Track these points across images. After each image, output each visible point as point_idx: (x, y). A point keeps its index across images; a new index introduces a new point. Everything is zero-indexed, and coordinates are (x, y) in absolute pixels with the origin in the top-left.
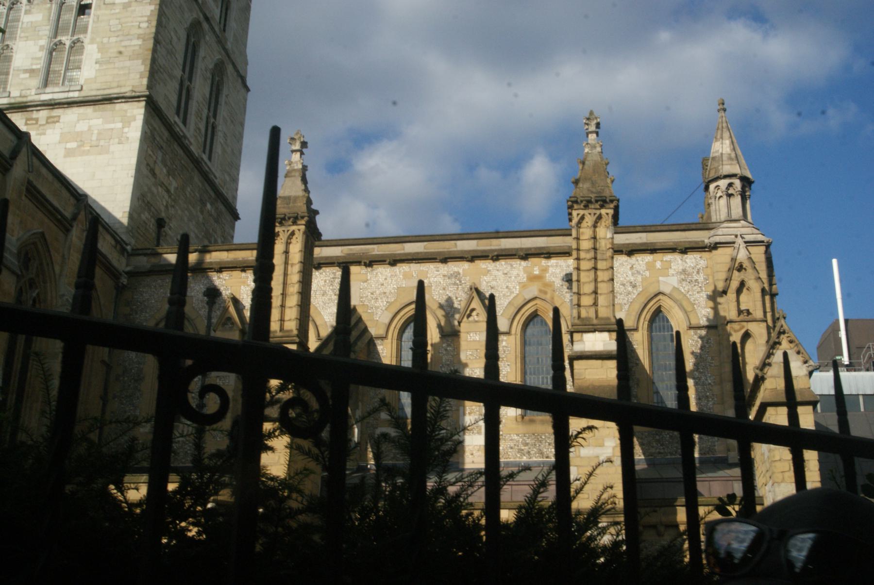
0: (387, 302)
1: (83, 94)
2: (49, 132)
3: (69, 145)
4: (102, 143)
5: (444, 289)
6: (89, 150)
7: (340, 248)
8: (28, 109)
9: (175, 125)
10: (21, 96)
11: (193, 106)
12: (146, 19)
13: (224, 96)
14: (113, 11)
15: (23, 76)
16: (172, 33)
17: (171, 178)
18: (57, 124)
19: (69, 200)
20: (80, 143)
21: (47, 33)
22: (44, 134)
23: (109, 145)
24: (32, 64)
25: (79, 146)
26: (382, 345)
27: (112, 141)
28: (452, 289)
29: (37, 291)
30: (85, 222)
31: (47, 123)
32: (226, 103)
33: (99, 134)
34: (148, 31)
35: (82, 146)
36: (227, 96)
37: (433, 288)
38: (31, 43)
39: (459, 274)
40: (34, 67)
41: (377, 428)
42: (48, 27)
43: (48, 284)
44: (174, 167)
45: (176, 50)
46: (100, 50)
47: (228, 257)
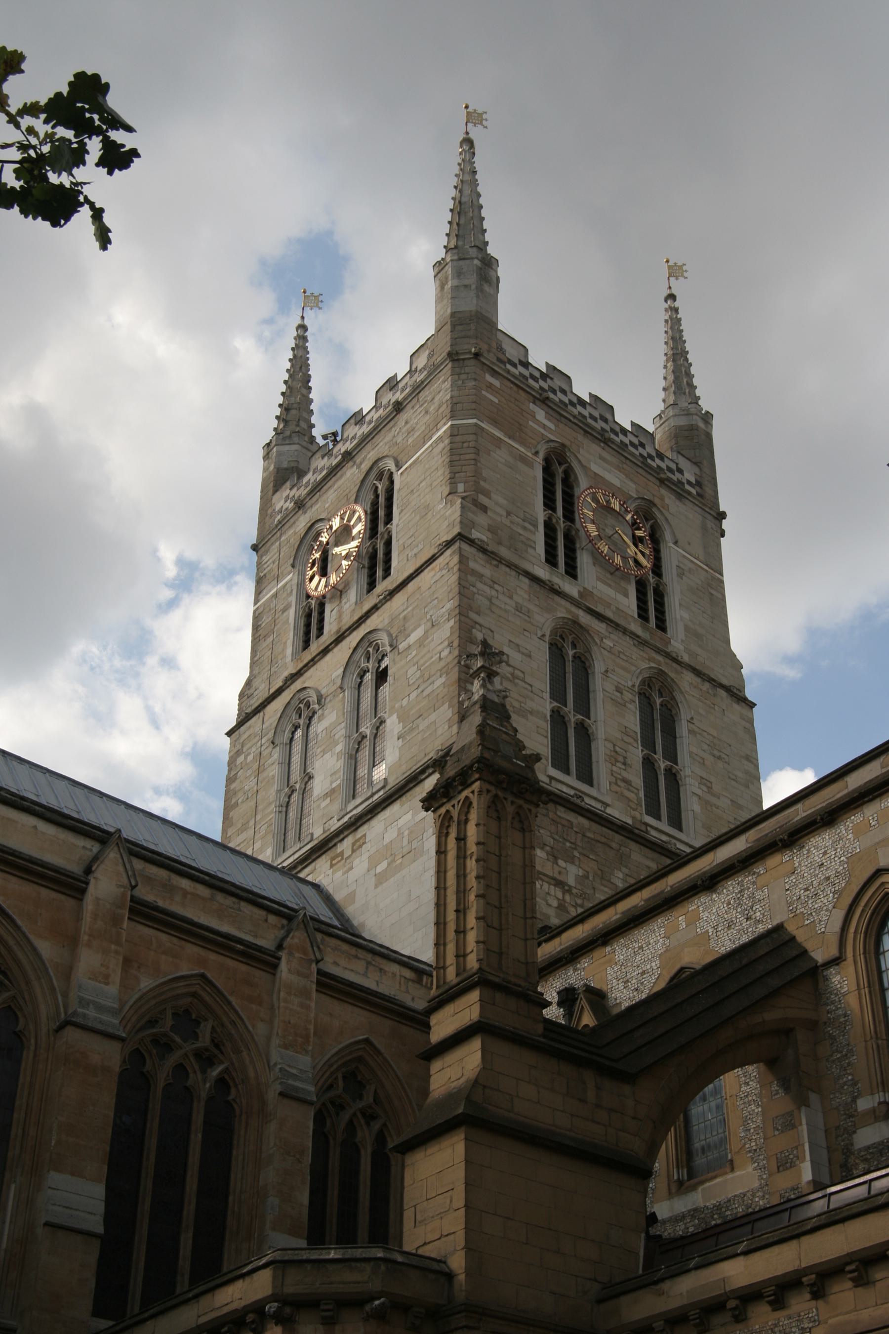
0: (834, 893)
1: (387, 788)
4: (415, 844)
6: (401, 862)
8: (331, 845)
9: (554, 783)
10: (324, 832)
11: (600, 750)
12: (446, 643)
13: (684, 723)
14: (410, 657)
15: (323, 804)
18: (364, 847)
20: (389, 860)
21: (343, 731)
23: (423, 842)
24: (332, 783)
25: (389, 864)
27: (425, 834)
30: (310, 949)
32: (691, 732)
33: (411, 833)
34: (451, 658)
35: (394, 861)
36: (690, 721)
38: (327, 756)
40: (334, 785)
42: (343, 724)
45: (523, 673)
47: (583, 932)
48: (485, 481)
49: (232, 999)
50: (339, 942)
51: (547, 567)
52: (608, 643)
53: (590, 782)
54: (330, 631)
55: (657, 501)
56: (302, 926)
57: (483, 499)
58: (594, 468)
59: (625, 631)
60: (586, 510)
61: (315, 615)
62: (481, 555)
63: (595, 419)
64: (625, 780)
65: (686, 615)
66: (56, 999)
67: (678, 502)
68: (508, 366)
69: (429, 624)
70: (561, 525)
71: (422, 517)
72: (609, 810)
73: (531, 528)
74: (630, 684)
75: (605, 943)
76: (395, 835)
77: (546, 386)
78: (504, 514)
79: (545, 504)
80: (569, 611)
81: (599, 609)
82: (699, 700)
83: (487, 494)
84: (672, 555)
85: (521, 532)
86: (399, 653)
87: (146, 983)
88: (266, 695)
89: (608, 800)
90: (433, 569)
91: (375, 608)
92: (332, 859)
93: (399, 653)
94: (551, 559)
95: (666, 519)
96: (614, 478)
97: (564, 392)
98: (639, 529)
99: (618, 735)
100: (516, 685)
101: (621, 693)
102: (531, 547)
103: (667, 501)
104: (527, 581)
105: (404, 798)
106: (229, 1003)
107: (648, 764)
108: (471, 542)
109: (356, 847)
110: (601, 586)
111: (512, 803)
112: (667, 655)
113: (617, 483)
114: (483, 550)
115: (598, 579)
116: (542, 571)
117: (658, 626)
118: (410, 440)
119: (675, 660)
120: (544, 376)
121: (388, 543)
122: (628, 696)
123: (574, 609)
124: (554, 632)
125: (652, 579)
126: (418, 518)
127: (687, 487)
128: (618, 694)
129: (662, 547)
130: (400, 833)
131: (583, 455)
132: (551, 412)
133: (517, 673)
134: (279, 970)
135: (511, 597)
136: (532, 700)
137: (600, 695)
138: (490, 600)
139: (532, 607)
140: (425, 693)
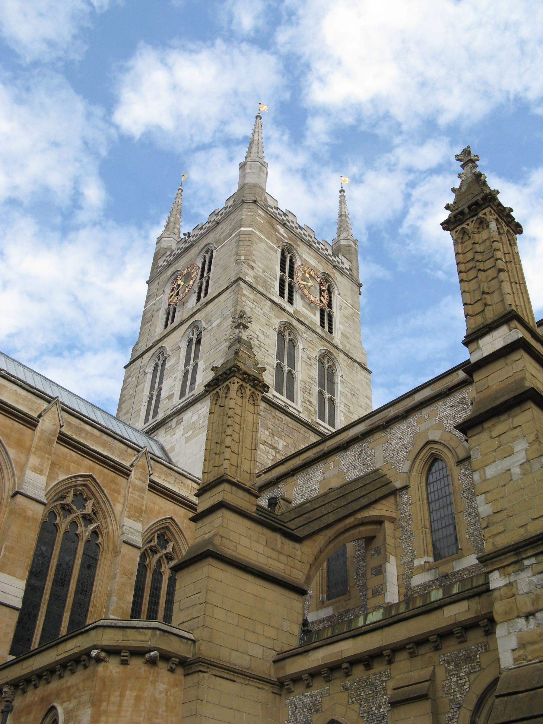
2: (177, 431)
3: (188, 434)
5: (454, 418)
7: (363, 424)
8: (167, 421)
9: (275, 399)
11: (298, 385)
12: (230, 327)
13: (339, 377)
16: (258, 333)
17: (276, 438)
19: (127, 451)
20: (193, 430)
22: (175, 434)
26: (407, 493)
28: (460, 416)
29: (94, 525)
30: (147, 468)
31: (177, 425)
35: (195, 431)
36: (342, 376)
37: (444, 422)
38: (169, 379)
39: (465, 398)
41: (412, 577)
43: (108, 519)
44: (280, 429)
46: (205, 362)
48: (254, 255)
49: (105, 490)
50: (162, 466)
51: (280, 297)
52: (305, 336)
53: (293, 401)
54: (177, 321)
55: (331, 275)
56: (144, 455)
57: (252, 264)
58: (304, 256)
59: (313, 331)
60: (299, 274)
61: (171, 314)
62: (249, 288)
63: (306, 236)
64: (309, 401)
65: (342, 327)
66: (14, 480)
67: (341, 276)
68: (269, 208)
69: (222, 318)
70: (287, 280)
71: (224, 270)
72: (301, 415)
73: (274, 279)
74: (314, 356)
75: (293, 475)
76: (197, 418)
77: (285, 219)
78: (262, 271)
79: (281, 270)
80: (288, 319)
81: (303, 320)
82: (346, 367)
83: (255, 262)
84: (336, 300)
85: (269, 280)
86: (207, 331)
87: (62, 477)
88: (145, 349)
89: (301, 410)
90: (227, 293)
91: (199, 310)
92: (166, 429)
93: (207, 331)
94: (282, 294)
95: (335, 283)
96: (313, 262)
97: (293, 222)
98: (323, 286)
99: (308, 380)
100: (261, 350)
101: (310, 360)
102: (273, 288)
103: (336, 275)
104: (269, 302)
105: (203, 400)
106: (103, 492)
107: (321, 393)
108: (245, 282)
109: (178, 423)
110: (304, 309)
111: (250, 390)
112: (333, 345)
113: (314, 265)
114: (250, 286)
115: (303, 306)
116: (277, 299)
117: (329, 331)
118: (222, 236)
119: (336, 347)
120: (285, 214)
121: (208, 282)
122: (313, 361)
123: (290, 318)
124: (280, 327)
125: (327, 310)
126: (222, 270)
127: (345, 270)
128: (309, 360)
129: (333, 295)
130: (199, 417)
131: (299, 250)
132: (286, 230)
133: (261, 344)
134: (130, 477)
135: (262, 309)
136: (268, 358)
137: (300, 359)
138: (252, 309)
139: (271, 315)
140: (218, 350)
